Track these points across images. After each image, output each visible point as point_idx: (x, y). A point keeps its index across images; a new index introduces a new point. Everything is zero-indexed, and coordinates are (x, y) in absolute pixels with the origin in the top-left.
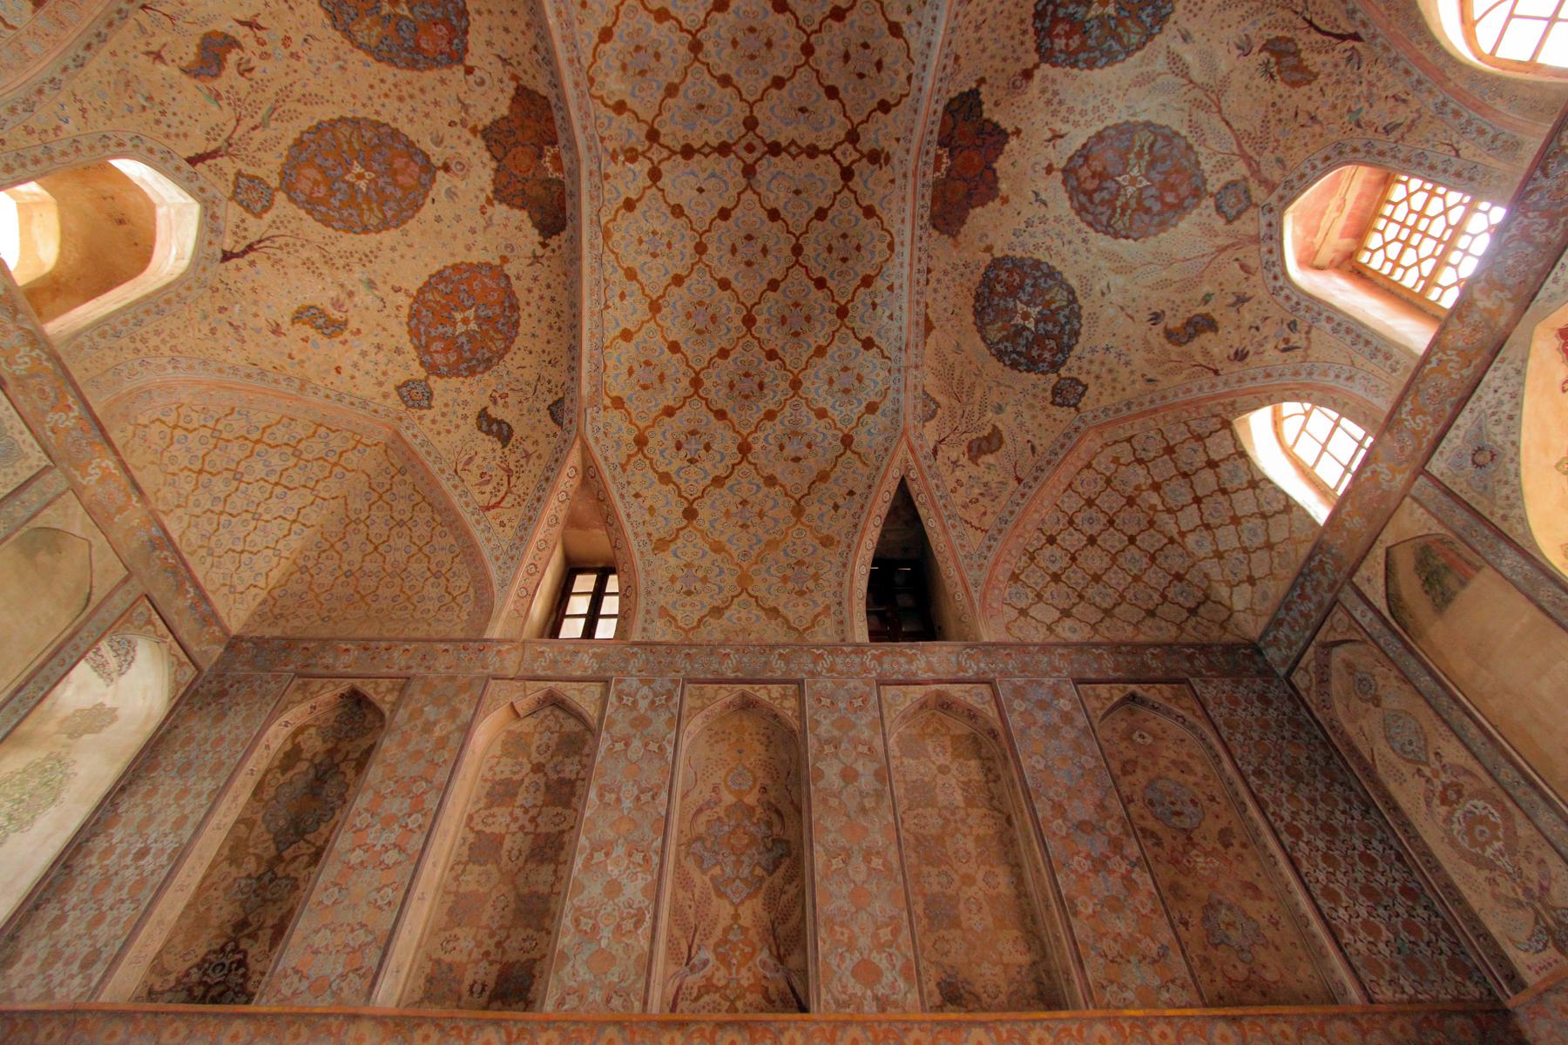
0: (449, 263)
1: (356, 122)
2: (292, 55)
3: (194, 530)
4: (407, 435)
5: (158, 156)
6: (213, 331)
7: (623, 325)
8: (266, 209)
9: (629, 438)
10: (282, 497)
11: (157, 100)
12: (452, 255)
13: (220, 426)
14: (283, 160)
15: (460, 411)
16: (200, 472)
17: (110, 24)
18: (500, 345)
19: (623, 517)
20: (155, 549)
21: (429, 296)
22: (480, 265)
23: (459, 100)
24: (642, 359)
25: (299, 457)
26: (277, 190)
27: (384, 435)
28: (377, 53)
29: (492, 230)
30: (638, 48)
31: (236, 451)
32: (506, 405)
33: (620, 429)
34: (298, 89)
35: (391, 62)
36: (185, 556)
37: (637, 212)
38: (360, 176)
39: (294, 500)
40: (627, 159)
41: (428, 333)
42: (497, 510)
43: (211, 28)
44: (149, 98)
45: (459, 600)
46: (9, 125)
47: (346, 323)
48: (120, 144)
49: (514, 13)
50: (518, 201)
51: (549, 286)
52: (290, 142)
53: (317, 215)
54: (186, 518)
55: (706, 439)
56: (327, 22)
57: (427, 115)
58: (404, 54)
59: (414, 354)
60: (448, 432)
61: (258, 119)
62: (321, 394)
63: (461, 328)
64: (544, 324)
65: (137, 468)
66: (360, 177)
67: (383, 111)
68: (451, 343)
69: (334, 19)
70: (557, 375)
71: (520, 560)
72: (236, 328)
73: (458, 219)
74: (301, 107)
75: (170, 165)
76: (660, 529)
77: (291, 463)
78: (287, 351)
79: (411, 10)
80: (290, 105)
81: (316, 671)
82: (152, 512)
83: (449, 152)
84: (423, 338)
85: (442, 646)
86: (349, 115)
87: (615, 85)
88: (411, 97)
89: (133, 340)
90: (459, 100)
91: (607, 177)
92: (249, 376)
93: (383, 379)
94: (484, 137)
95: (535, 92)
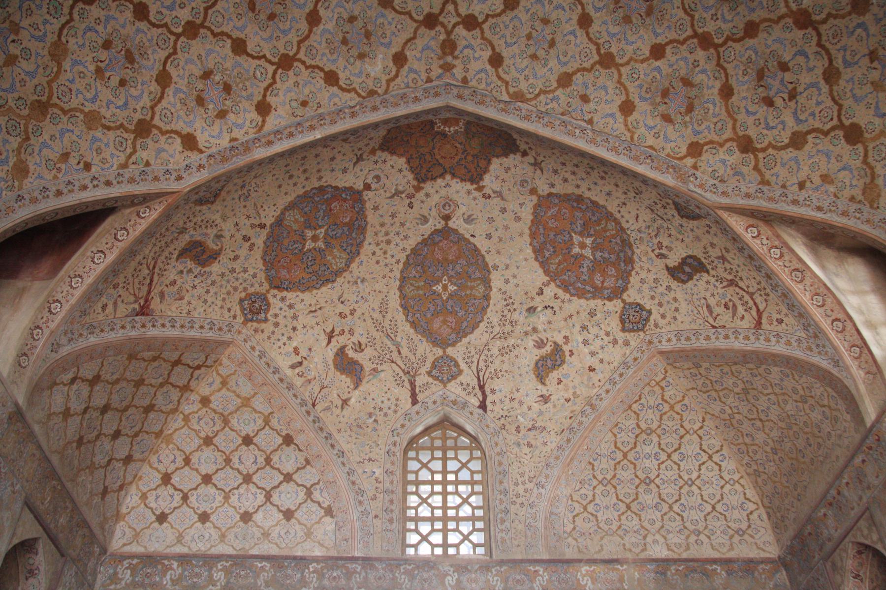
0: (528, 240)
1: (403, 279)
2: (351, 314)
3: (671, 535)
4: (665, 346)
5: (407, 422)
6: (529, 445)
7: (614, 108)
8: (457, 365)
9: (737, 156)
10: (683, 457)
11: (372, 410)
12: (521, 235)
13: (600, 477)
14: (424, 339)
15: (662, 289)
16: (628, 507)
17: (321, 429)
18: (611, 225)
19: (819, 215)
20: (664, 574)
21: (553, 267)
22: (535, 214)
23: (392, 197)
24: (658, 99)
25: (653, 431)
26: (444, 352)
27: (660, 364)
28: (353, 254)
29: (505, 193)
30: (345, 42)
31: (626, 474)
32: (669, 249)
33: (724, 162)
34: (376, 315)
35: (360, 245)
36: (685, 556)
37: (504, 54)
38: (445, 288)
39: (691, 447)
40: (452, 53)
41: (584, 282)
42: (765, 316)
43: (331, 363)
44: (370, 415)
45: (833, 405)
46: (368, 507)
47: (555, 343)
48: (395, 444)
49: (317, 156)
50: (483, 163)
51: (564, 164)
52: (412, 331)
53: (468, 330)
54: (658, 537)
55: (772, 64)
56: (330, 285)
57: (402, 224)
58: (354, 235)
59: (599, 302)
60: (677, 310)
61: (393, 348)
62: (604, 395)
63: (587, 252)
64: (600, 182)
65: (600, 551)
66: (445, 288)
67: (397, 257)
68: (597, 266)
69: (328, 281)
70: (650, 196)
71: (821, 331)
72: (533, 428)
73: (491, 220)
74: (389, 316)
75: (414, 415)
76: (851, 183)
77: (655, 439)
78: (562, 401)
79: (321, 227)
80: (386, 324)
81: (829, 546)
82: (635, 561)
83: (434, 212)
84: (588, 288)
85: (858, 460)
86: (398, 283)
87: (378, 67)
88: (387, 234)
89: (514, 503)
90: (392, 197)
91: (465, 81)
92: (569, 441)
93: (612, 338)
94: (424, 181)
95: (385, 137)
